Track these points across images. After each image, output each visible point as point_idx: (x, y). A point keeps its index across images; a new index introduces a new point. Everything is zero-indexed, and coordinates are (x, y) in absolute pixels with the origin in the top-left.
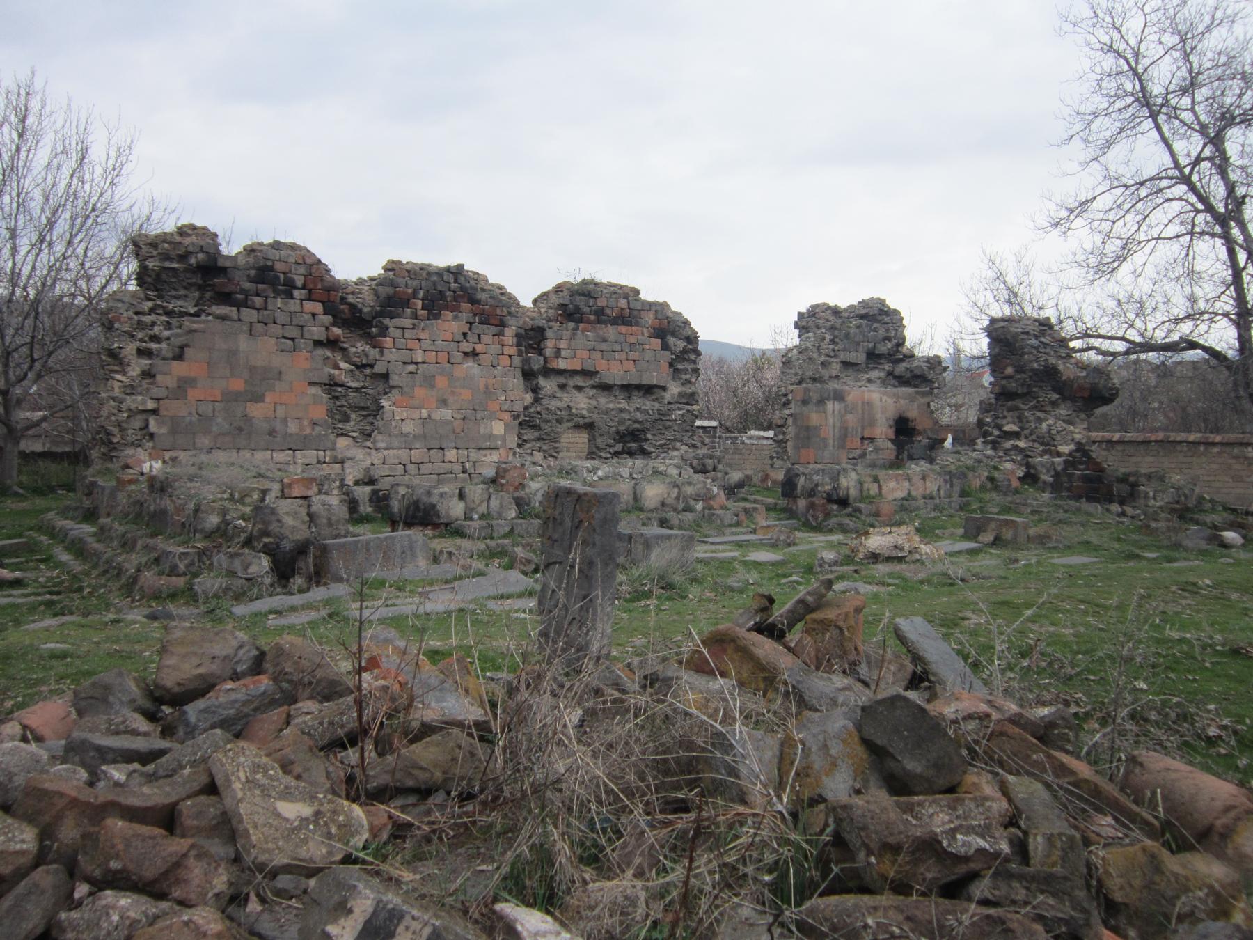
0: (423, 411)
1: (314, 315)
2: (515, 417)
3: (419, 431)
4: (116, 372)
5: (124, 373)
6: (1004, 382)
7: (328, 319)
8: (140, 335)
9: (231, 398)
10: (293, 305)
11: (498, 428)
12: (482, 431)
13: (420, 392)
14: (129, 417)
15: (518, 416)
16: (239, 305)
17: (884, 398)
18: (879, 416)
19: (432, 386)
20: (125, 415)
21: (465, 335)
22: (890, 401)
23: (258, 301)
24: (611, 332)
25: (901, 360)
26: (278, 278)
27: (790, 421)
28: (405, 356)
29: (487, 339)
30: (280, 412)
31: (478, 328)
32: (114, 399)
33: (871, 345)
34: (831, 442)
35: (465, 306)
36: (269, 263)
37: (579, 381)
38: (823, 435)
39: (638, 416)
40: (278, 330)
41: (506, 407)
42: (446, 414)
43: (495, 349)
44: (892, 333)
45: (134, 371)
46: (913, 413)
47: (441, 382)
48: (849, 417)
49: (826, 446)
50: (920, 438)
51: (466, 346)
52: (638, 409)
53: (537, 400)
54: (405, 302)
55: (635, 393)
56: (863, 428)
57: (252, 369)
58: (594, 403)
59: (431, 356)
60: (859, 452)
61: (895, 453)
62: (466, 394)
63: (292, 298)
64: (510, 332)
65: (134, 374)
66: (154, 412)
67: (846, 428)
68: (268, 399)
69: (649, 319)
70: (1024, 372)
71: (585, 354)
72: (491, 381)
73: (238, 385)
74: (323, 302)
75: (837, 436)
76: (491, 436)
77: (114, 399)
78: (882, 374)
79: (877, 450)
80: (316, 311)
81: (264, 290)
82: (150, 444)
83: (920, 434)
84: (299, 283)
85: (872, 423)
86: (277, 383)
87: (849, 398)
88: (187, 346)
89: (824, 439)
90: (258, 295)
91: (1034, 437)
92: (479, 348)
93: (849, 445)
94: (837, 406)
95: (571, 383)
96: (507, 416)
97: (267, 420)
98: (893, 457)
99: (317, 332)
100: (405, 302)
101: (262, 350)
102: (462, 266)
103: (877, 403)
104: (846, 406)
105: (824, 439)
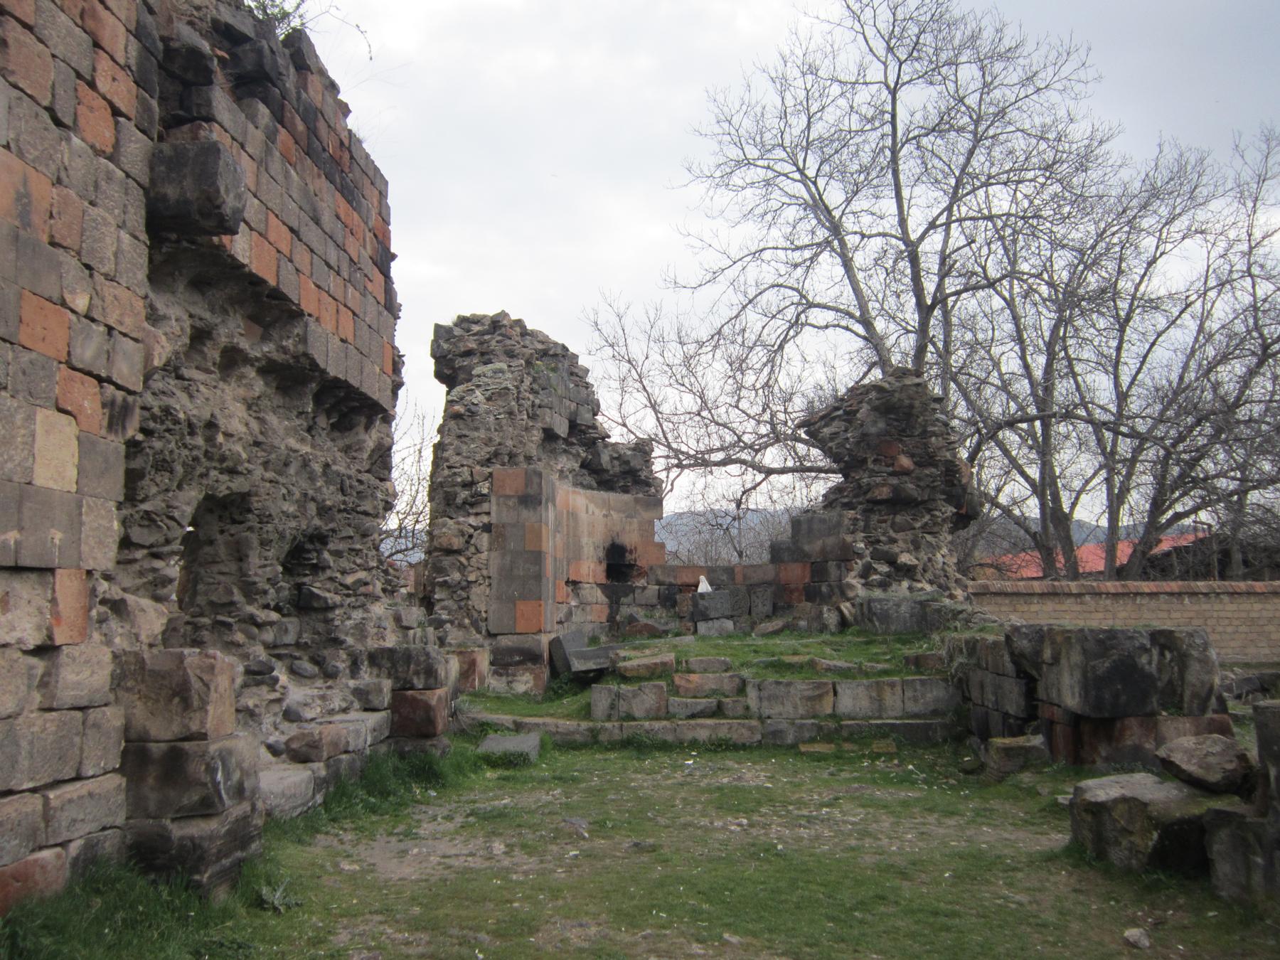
2: (117, 416)
6: (894, 481)
17: (592, 507)
18: (584, 540)
22: (599, 513)
46: (630, 539)
50: (641, 582)
61: (606, 611)
70: (935, 465)
79: (583, 604)
83: (642, 573)
96: (88, 399)
98: (604, 619)
103: (583, 516)
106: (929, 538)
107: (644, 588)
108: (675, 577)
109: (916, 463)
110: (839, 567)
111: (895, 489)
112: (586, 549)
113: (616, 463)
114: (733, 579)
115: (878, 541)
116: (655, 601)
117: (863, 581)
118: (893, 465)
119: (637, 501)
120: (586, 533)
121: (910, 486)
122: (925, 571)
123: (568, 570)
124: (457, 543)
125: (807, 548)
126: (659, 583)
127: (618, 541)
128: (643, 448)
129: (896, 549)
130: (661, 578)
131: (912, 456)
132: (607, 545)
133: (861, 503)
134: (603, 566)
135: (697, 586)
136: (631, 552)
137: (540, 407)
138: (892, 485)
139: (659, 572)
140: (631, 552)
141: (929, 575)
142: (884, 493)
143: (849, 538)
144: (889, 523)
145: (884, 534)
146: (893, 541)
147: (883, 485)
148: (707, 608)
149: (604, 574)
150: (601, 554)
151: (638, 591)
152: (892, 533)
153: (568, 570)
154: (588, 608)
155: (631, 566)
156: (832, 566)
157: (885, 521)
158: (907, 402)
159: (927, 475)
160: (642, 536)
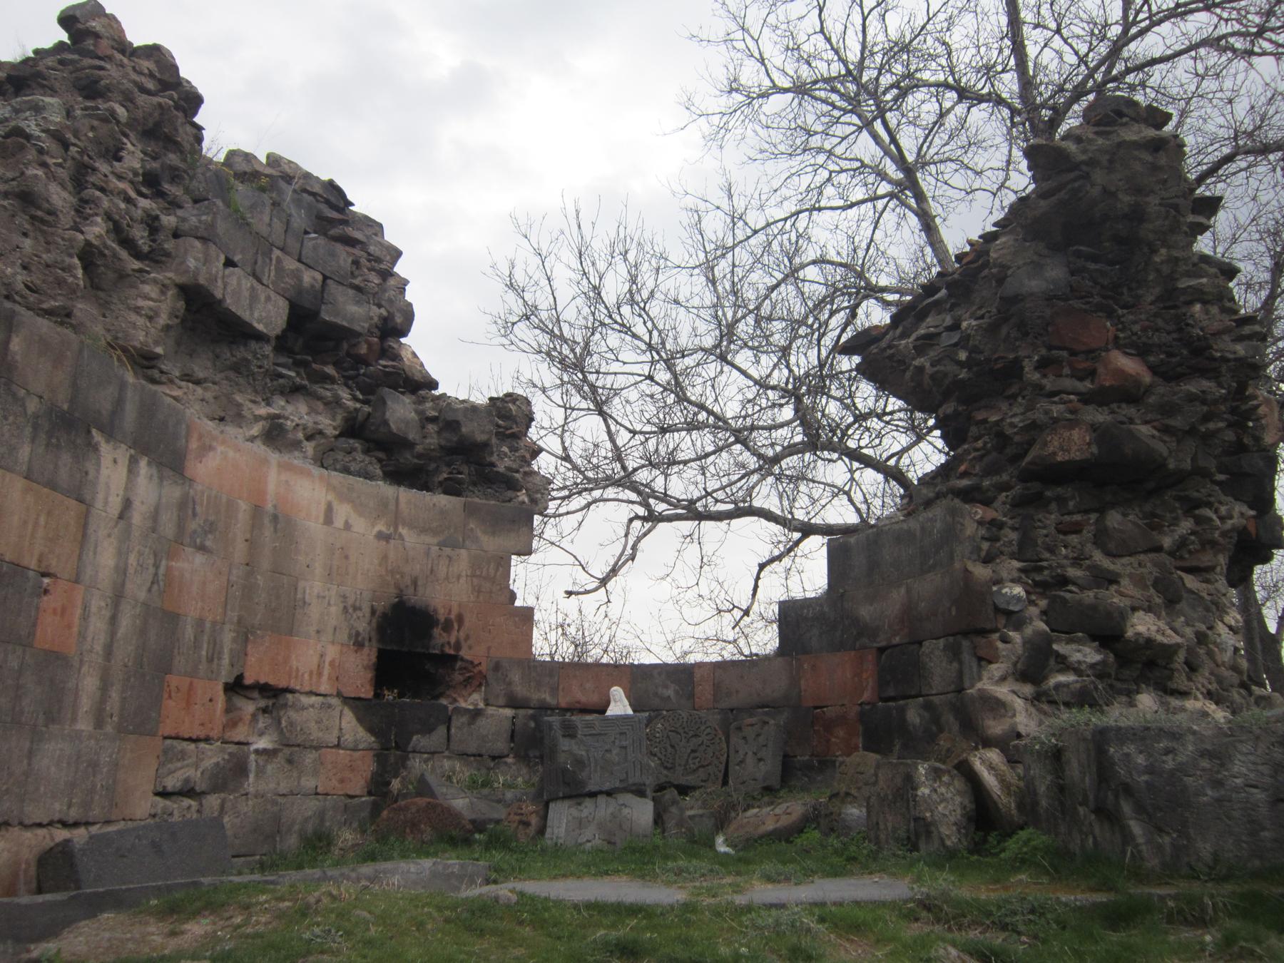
6: (1101, 416)
17: (343, 512)
18: (313, 587)
33: (310, 278)
38: (48, 631)
46: (447, 593)
48: (192, 565)
49: (55, 708)
50: (474, 700)
56: (245, 634)
60: (213, 756)
61: (367, 766)
67: (172, 619)
75: (125, 652)
78: (328, 424)
79: (291, 748)
83: (474, 679)
85: (284, 618)
93: (175, 717)
94: (148, 488)
98: (357, 785)
104: (186, 506)
106: (1191, 581)
107: (476, 714)
108: (554, 690)
109: (1153, 369)
110: (954, 653)
112: (314, 611)
113: (432, 428)
114: (691, 696)
115: (1064, 581)
116: (501, 745)
117: (1028, 689)
118: (1092, 374)
119: (470, 511)
120: (318, 569)
121: (1145, 430)
122: (1192, 668)
123: (240, 655)
125: (866, 612)
126: (514, 703)
127: (414, 599)
128: (510, 415)
129: (1115, 600)
130: (520, 690)
131: (1141, 351)
132: (381, 606)
133: (1004, 487)
134: (369, 655)
135: (604, 711)
136: (447, 626)
137: (176, 235)
138: (1094, 427)
139: (516, 676)
140: (447, 626)
141: (1203, 679)
142: (1072, 444)
143: (981, 572)
144: (1088, 533)
145: (1077, 561)
146: (1111, 579)
147: (1072, 424)
148: (580, 763)
149: (370, 675)
150: (363, 625)
151: (458, 721)
152: (1098, 557)
153: (240, 655)
154: (309, 758)
155: (449, 660)
156: (934, 655)
157: (1076, 529)
159: (1191, 398)
160: (479, 591)
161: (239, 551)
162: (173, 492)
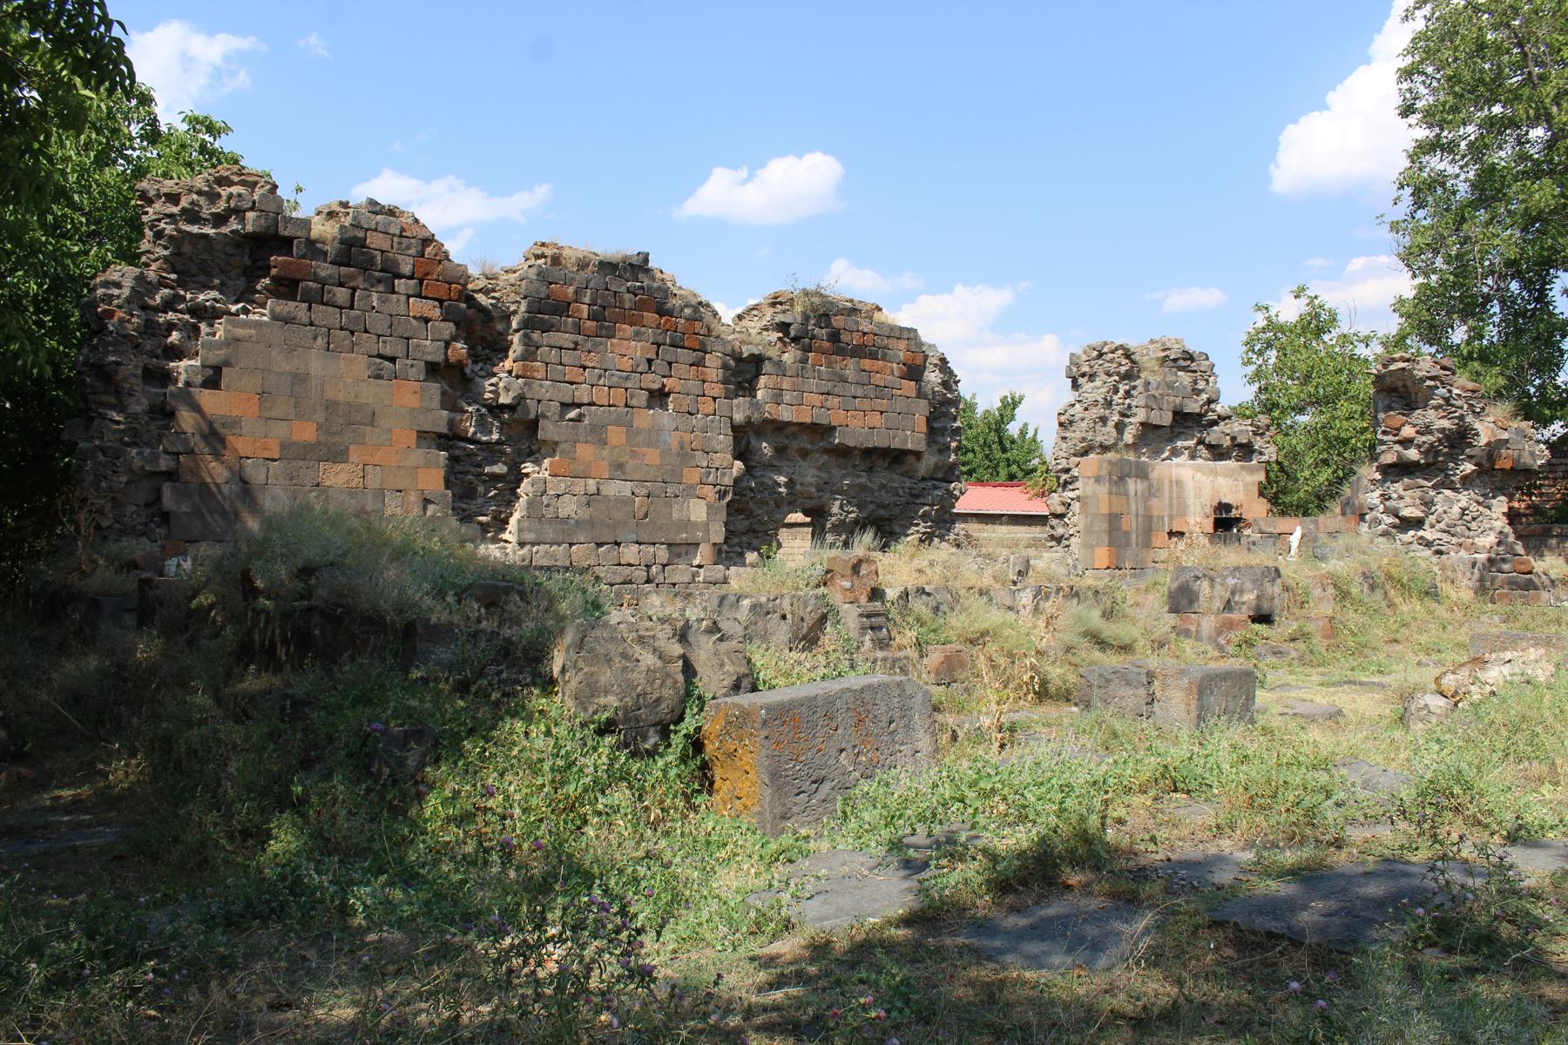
0: (591, 482)
1: (427, 320)
3: (584, 514)
4: (111, 407)
5: (121, 409)
7: (448, 328)
8: (148, 345)
9: (294, 452)
10: (396, 303)
11: (698, 511)
12: (675, 515)
13: (584, 451)
14: (128, 483)
15: (725, 493)
16: (310, 300)
17: (1199, 476)
19: (603, 443)
20: (124, 479)
21: (650, 361)
23: (342, 294)
24: (850, 367)
25: (1214, 423)
26: (374, 257)
27: (1076, 506)
28: (566, 394)
29: (681, 369)
30: (374, 481)
31: (668, 353)
32: (104, 451)
34: (1134, 537)
35: (650, 317)
36: (361, 234)
37: (804, 442)
39: (885, 498)
40: (368, 342)
41: (711, 479)
42: (617, 488)
43: (694, 386)
44: (1201, 385)
45: (139, 406)
47: (616, 435)
49: (1128, 544)
50: (1247, 532)
51: (653, 381)
52: (883, 486)
53: (749, 469)
54: (561, 308)
55: (880, 462)
56: (1171, 518)
57: (330, 406)
58: (824, 475)
59: (600, 395)
62: (652, 456)
63: (393, 292)
64: (713, 361)
65: (139, 409)
66: (171, 475)
68: (354, 456)
69: (900, 350)
70: (1431, 433)
71: (817, 399)
72: (687, 437)
73: (307, 433)
74: (441, 302)
76: (687, 524)
77: (104, 451)
80: (429, 315)
81: (352, 277)
82: (163, 531)
83: (1249, 525)
84: (406, 269)
86: (368, 429)
87: (1154, 475)
88: (228, 364)
89: (1127, 533)
90: (341, 285)
91: (1442, 525)
92: (670, 383)
95: (795, 445)
97: (352, 492)
99: (430, 348)
100: (561, 308)
101: (344, 374)
102: (646, 258)
104: (1150, 486)
105: (1127, 533)
111: (1400, 456)
112: (1192, 508)
124: (1060, 510)
130: (1265, 528)
132: (1215, 503)
150: (1209, 510)
158: (1400, 383)
161: (1167, 495)
162: (1146, 484)
